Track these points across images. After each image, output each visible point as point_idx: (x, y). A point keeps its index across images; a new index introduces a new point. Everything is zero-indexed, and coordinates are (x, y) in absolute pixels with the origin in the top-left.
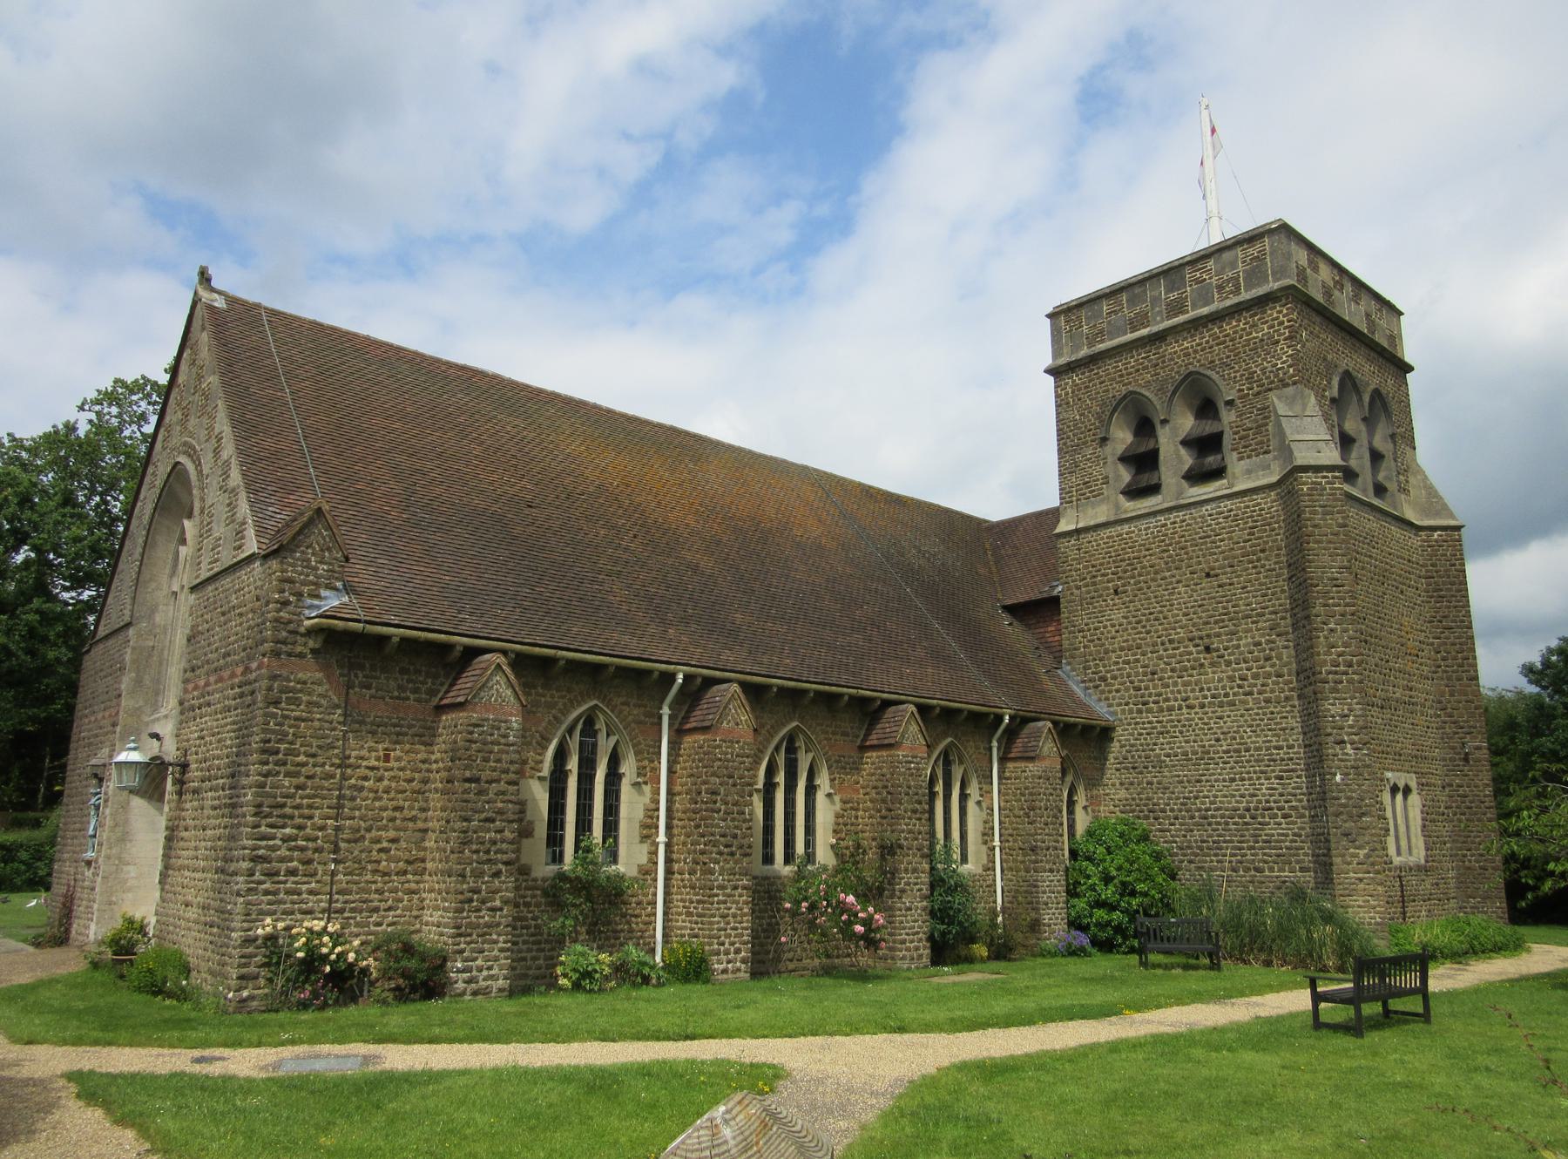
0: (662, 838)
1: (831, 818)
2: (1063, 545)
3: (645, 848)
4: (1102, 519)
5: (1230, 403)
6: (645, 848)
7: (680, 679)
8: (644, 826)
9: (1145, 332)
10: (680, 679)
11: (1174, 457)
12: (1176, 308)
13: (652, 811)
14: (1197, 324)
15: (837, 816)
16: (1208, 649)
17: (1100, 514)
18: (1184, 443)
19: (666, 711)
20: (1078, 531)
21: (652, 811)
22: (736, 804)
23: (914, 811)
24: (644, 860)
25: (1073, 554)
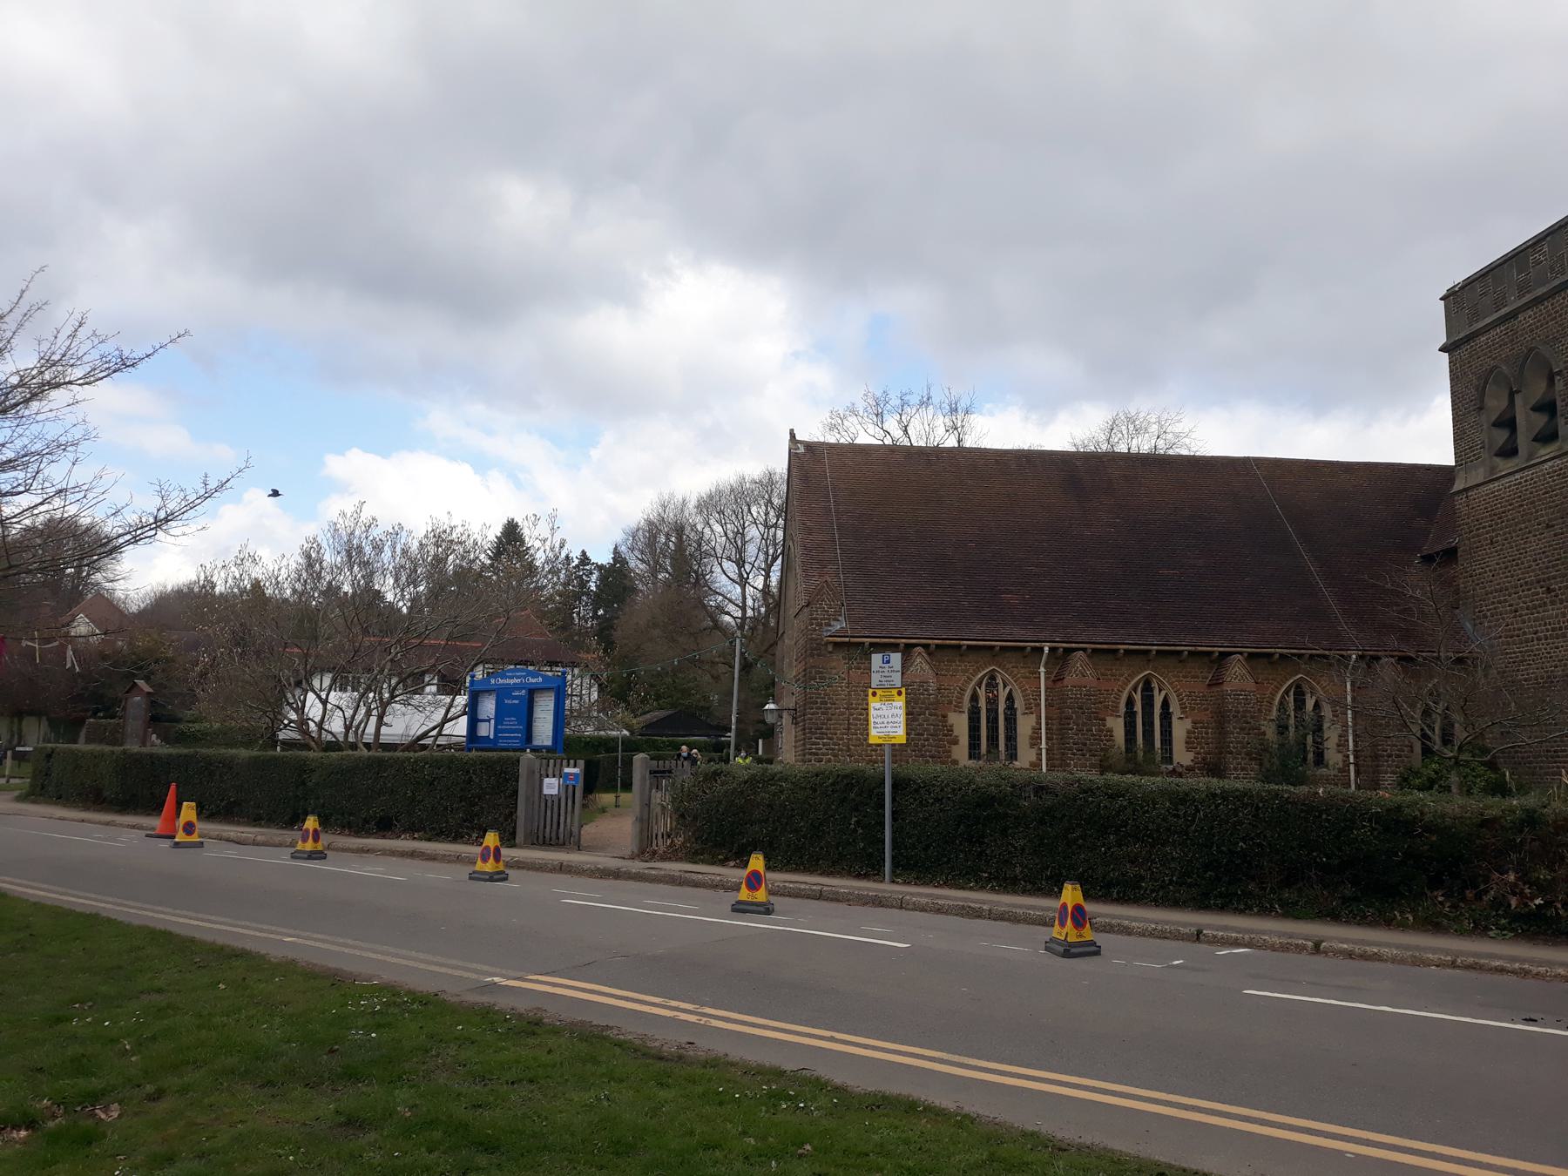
0: (1043, 746)
1: (1184, 734)
2: (1460, 501)
3: (1034, 752)
4: (1481, 480)
5: (1559, 373)
6: (1034, 752)
7: (1046, 650)
8: (1032, 738)
9: (1503, 311)
10: (1046, 650)
11: (1528, 422)
12: (1523, 289)
13: (1037, 730)
14: (1538, 301)
15: (1188, 732)
16: (1549, 590)
17: (1479, 475)
18: (1534, 409)
19: (1042, 669)
20: (1466, 490)
21: (1037, 730)
22: (1084, 724)
23: (1242, 729)
24: (1033, 758)
25: (1465, 510)
